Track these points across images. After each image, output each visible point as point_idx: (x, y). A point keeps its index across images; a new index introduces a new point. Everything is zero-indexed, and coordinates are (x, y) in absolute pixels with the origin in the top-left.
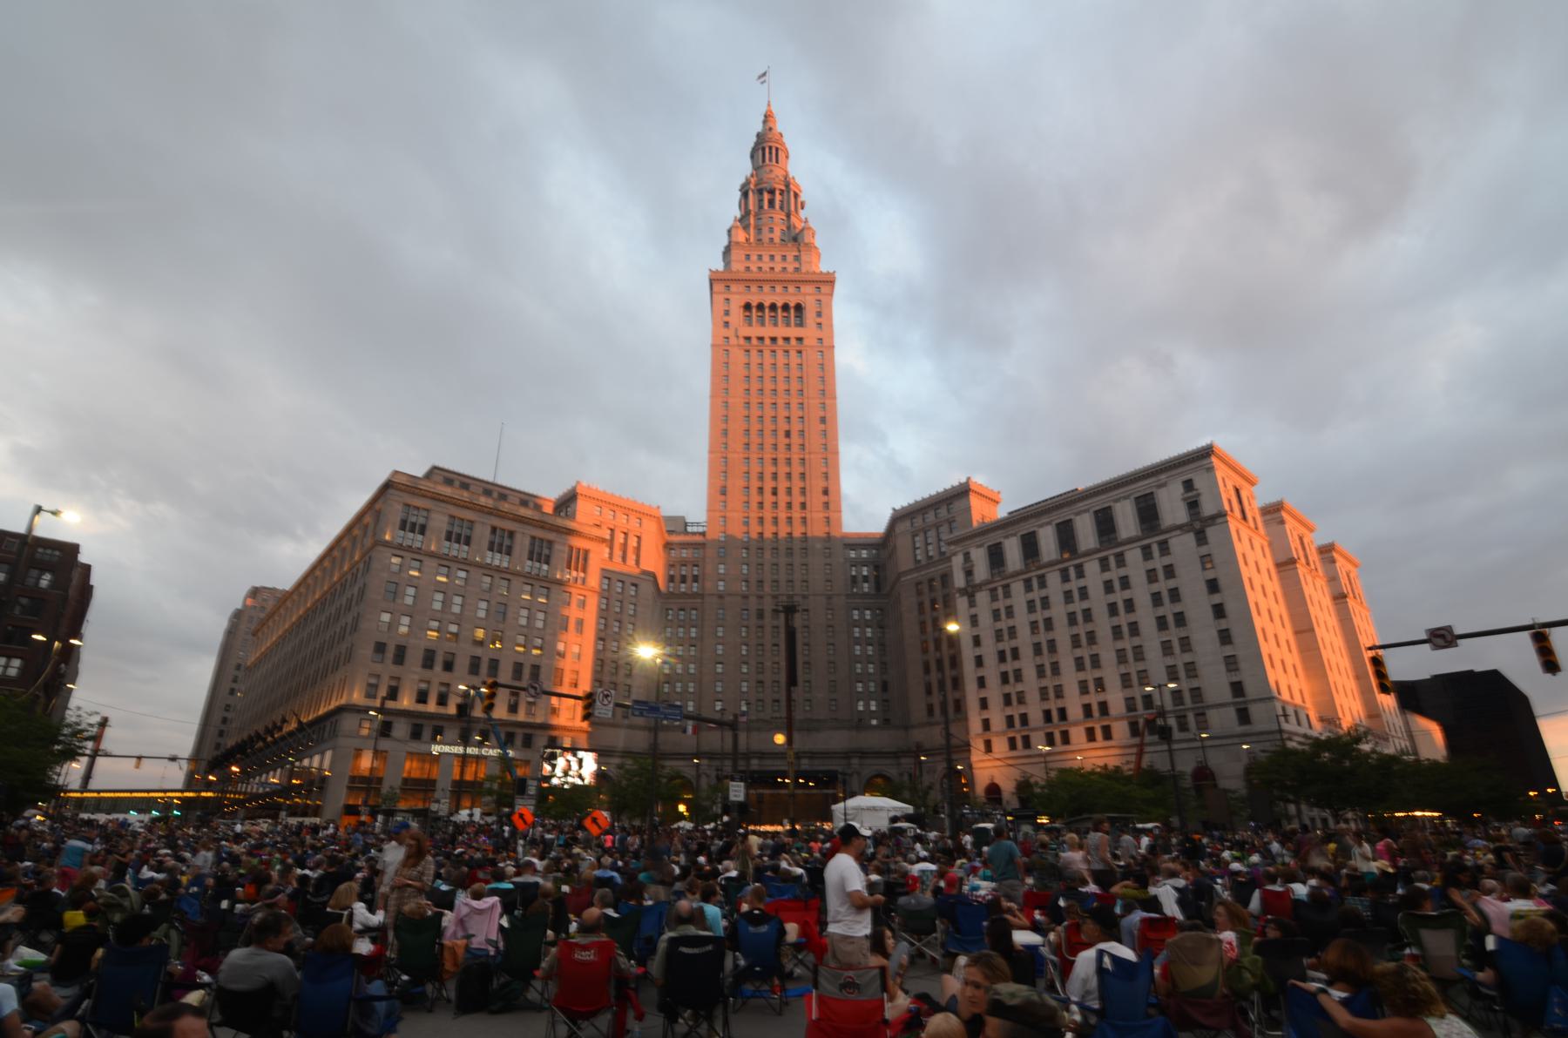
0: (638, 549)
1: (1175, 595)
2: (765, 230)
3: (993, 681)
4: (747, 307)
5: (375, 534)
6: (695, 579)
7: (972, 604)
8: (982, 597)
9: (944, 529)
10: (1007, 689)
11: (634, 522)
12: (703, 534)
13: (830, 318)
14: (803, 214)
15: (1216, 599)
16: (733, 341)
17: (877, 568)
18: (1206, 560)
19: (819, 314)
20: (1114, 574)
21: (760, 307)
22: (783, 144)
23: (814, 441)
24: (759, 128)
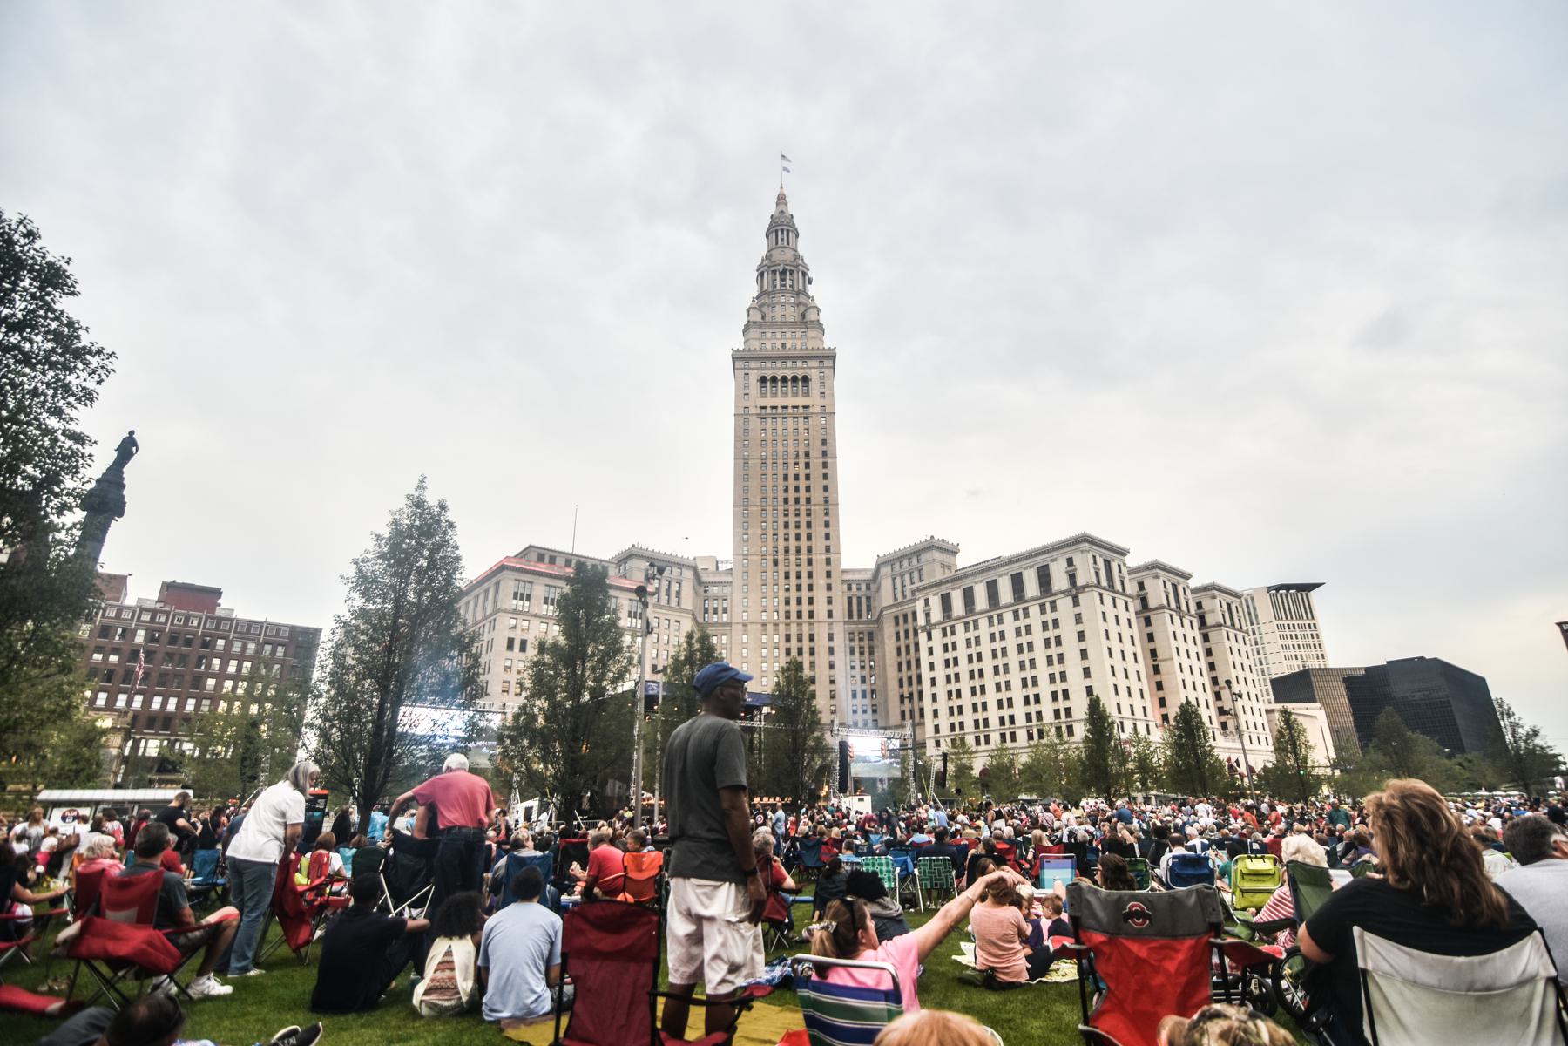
0: (678, 592)
1: (1058, 641)
2: (778, 307)
3: (942, 697)
4: (763, 380)
5: (495, 602)
6: (725, 610)
7: (930, 638)
8: (937, 633)
9: (916, 575)
10: (951, 704)
11: (676, 571)
12: (730, 572)
13: (832, 388)
14: (811, 290)
15: (1083, 645)
16: (753, 410)
17: (868, 599)
18: (1078, 619)
19: (822, 383)
20: (1022, 623)
21: (774, 379)
22: (793, 225)
23: (817, 495)
24: (773, 210)
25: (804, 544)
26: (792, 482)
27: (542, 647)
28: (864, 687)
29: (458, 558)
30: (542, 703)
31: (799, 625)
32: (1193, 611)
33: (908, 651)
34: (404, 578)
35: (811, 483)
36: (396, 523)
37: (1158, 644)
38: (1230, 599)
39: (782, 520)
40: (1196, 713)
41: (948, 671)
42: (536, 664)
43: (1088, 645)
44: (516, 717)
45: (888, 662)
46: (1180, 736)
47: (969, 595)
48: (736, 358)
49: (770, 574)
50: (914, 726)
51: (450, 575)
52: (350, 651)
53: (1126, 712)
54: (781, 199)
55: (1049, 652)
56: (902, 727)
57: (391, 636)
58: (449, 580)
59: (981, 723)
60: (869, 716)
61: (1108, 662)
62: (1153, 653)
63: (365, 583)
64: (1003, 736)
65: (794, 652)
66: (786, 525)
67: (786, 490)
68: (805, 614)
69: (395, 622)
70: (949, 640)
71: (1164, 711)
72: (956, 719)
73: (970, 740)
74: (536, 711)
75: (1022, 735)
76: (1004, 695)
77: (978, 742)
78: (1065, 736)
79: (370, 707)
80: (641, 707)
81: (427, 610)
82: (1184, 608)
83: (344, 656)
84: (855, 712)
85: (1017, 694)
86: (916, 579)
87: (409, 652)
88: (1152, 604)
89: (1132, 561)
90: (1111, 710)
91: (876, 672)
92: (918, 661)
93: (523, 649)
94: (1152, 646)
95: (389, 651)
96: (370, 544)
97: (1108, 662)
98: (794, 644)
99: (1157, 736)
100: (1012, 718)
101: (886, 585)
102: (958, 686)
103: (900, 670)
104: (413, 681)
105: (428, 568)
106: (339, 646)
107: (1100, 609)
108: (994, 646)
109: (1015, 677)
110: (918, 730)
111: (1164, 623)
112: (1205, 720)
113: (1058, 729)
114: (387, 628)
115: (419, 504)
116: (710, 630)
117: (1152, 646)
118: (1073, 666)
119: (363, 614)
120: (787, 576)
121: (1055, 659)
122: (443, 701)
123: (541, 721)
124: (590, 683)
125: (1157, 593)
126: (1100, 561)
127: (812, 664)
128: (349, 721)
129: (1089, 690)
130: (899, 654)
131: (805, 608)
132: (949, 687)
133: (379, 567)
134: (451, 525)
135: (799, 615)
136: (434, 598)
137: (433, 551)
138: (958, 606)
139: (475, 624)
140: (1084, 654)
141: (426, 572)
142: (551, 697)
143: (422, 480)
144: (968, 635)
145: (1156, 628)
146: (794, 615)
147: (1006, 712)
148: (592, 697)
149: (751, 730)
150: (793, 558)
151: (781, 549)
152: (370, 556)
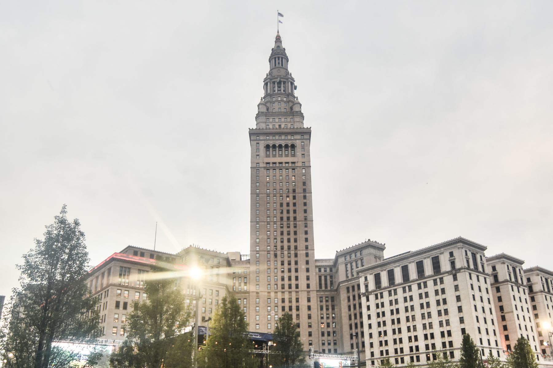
25: (292, 244)
26: (285, 207)
27: (136, 306)
28: (329, 330)
29: (86, 254)
30: (136, 340)
31: (290, 292)
32: (525, 283)
33: (355, 308)
34: (54, 266)
35: (297, 208)
36: (49, 233)
37: (504, 303)
38: (547, 276)
39: (279, 230)
40: (527, 344)
41: (379, 320)
42: (133, 317)
43: (463, 303)
44: (121, 349)
45: (343, 314)
46: (518, 358)
47: (391, 274)
48: (253, 134)
49: (272, 262)
50: (359, 352)
51: (81, 264)
52: (22, 309)
53: (485, 344)
54: (278, 39)
55: (439, 308)
56: (352, 353)
57: (46, 300)
58: (80, 268)
59: (399, 351)
60: (332, 347)
61: (474, 314)
62: (502, 308)
63: (30, 269)
64: (412, 358)
65: (287, 309)
66: (282, 233)
67: (282, 213)
68: (293, 286)
69: (48, 292)
70: (379, 301)
71: (508, 343)
72: (384, 348)
73: (392, 361)
74: (133, 345)
75: (423, 357)
76: (412, 334)
77: (397, 362)
78: (449, 358)
79: (34, 343)
80: (195, 342)
81: (67, 285)
82: (520, 281)
83: (18, 312)
84: (323, 344)
85: (420, 333)
86: (359, 265)
87: (57, 310)
88: (501, 279)
89: (488, 254)
90: (477, 343)
91: (336, 320)
92: (361, 314)
93: (125, 307)
94: (500, 304)
95: (45, 309)
96: (34, 246)
97: (474, 314)
98: (287, 304)
99: (504, 358)
100: (417, 348)
101: (342, 268)
102: (385, 328)
103: (350, 319)
104: (59, 327)
105: (68, 260)
106: (15, 306)
107: (469, 282)
108: (406, 304)
109: (419, 323)
110: (361, 355)
111: (508, 290)
112: (533, 348)
113: (445, 354)
114: (44, 296)
115: (62, 222)
116: (237, 296)
117: (500, 304)
118: (454, 317)
119: (29, 287)
120: (282, 264)
121: (443, 312)
122: (77, 339)
123: (136, 351)
124: (165, 328)
125: (503, 273)
126: (469, 254)
127: (298, 316)
128: (21, 351)
129: (463, 331)
130: (350, 310)
131: (293, 282)
132: (380, 329)
133: (38, 259)
134: (82, 234)
135: (290, 287)
136: (72, 278)
137: (71, 250)
138: (385, 282)
139: (96, 293)
140: (460, 309)
141: (67, 262)
142: (142, 336)
143: (64, 207)
144: (391, 298)
145: (503, 293)
146: (286, 287)
147: (414, 344)
148: (166, 336)
149: (261, 355)
150: (286, 253)
151: (279, 248)
152: (34, 253)
